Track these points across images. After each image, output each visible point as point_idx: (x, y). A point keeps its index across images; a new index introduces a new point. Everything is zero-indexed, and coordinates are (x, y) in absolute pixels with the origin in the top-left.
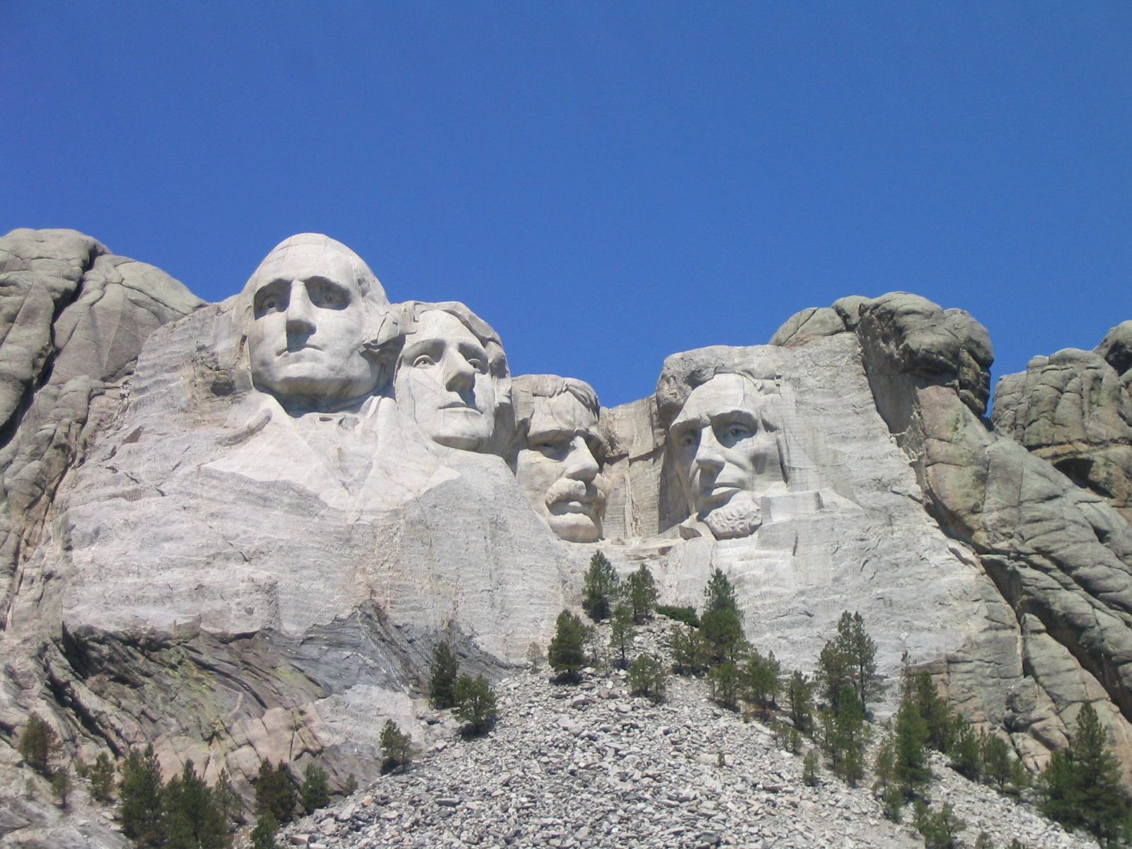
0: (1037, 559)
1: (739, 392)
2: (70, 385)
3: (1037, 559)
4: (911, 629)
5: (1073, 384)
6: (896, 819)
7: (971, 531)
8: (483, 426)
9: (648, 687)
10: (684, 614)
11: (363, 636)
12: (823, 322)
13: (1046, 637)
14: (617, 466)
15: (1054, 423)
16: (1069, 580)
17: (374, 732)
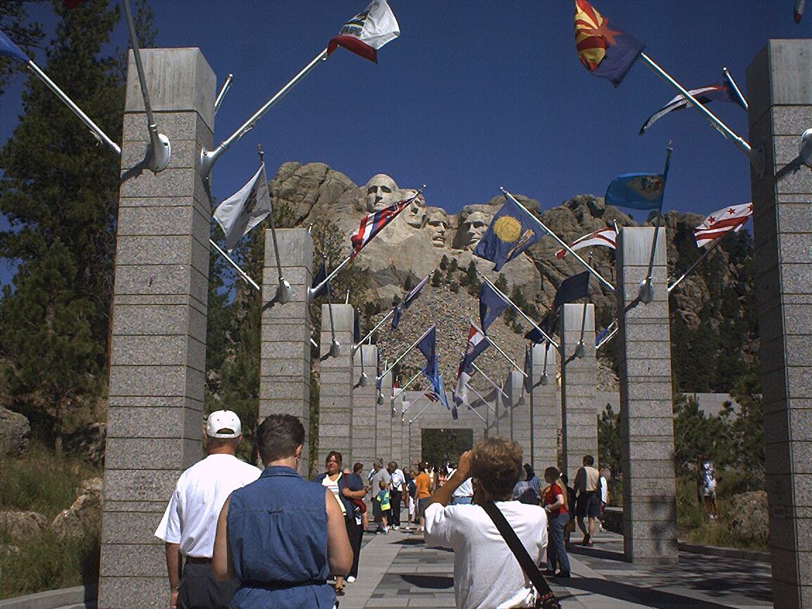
0: (547, 262)
1: (480, 217)
2: (324, 206)
3: (547, 262)
4: (516, 276)
5: (561, 216)
6: (507, 324)
7: (532, 254)
8: (419, 221)
9: (454, 289)
10: (463, 269)
11: (390, 272)
12: (502, 200)
13: (548, 282)
14: (449, 230)
15: (556, 226)
16: (554, 268)
17: (392, 296)
